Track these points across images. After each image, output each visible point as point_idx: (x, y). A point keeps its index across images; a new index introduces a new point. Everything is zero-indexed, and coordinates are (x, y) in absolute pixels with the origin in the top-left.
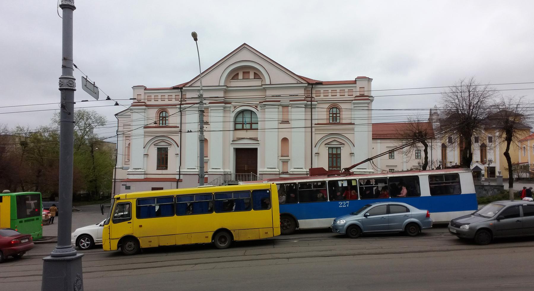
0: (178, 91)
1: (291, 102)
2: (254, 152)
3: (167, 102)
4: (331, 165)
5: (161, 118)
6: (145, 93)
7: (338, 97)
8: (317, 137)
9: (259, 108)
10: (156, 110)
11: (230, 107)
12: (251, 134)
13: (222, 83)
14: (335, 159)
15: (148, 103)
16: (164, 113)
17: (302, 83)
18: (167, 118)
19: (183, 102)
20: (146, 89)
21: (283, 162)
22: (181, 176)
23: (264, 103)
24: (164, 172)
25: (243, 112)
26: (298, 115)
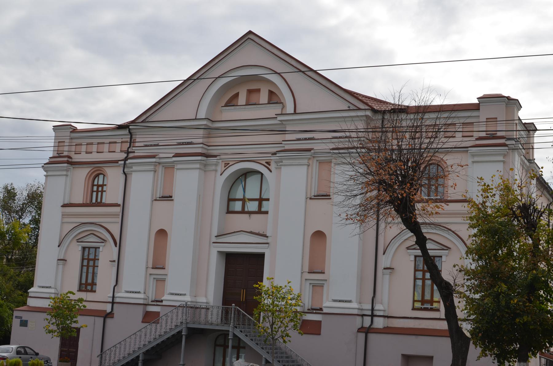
4: (418, 297)
5: (95, 188)
9: (273, 166)
11: (216, 165)
13: (202, 114)
15: (77, 158)
16: (101, 177)
17: (359, 109)
19: (131, 155)
20: (75, 130)
22: (115, 305)
25: (245, 174)
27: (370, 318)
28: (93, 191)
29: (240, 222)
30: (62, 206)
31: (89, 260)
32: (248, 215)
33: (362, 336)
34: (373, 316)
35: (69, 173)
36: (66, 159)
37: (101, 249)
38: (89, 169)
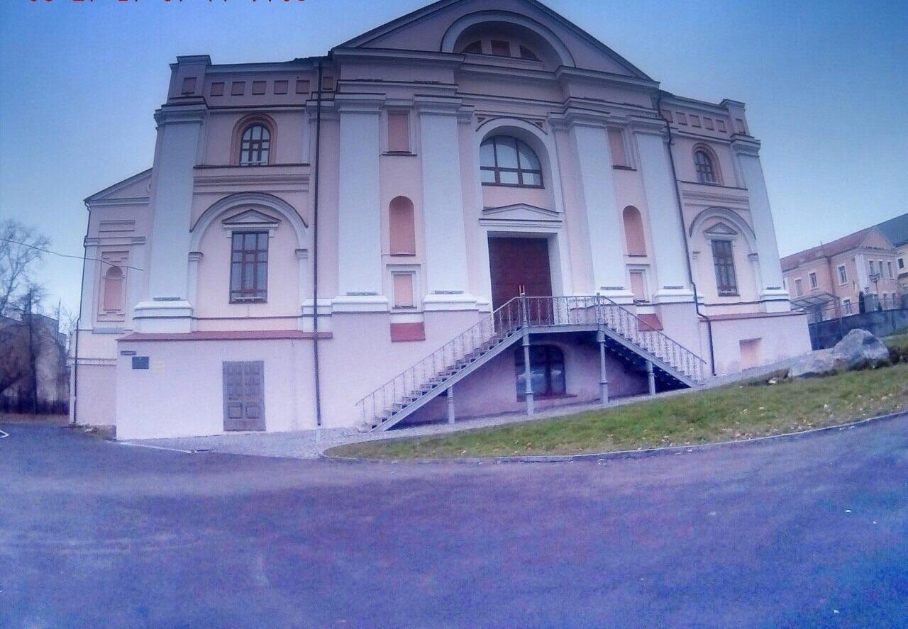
1: (635, 119)
3: (269, 99)
5: (246, 146)
6: (207, 75)
8: (689, 215)
10: (238, 118)
14: (723, 268)
18: (265, 145)
21: (633, 273)
22: (321, 321)
24: (255, 310)
28: (242, 150)
29: (501, 197)
31: (245, 252)
33: (704, 326)
36: (201, 100)
37: (271, 233)
38: (241, 116)
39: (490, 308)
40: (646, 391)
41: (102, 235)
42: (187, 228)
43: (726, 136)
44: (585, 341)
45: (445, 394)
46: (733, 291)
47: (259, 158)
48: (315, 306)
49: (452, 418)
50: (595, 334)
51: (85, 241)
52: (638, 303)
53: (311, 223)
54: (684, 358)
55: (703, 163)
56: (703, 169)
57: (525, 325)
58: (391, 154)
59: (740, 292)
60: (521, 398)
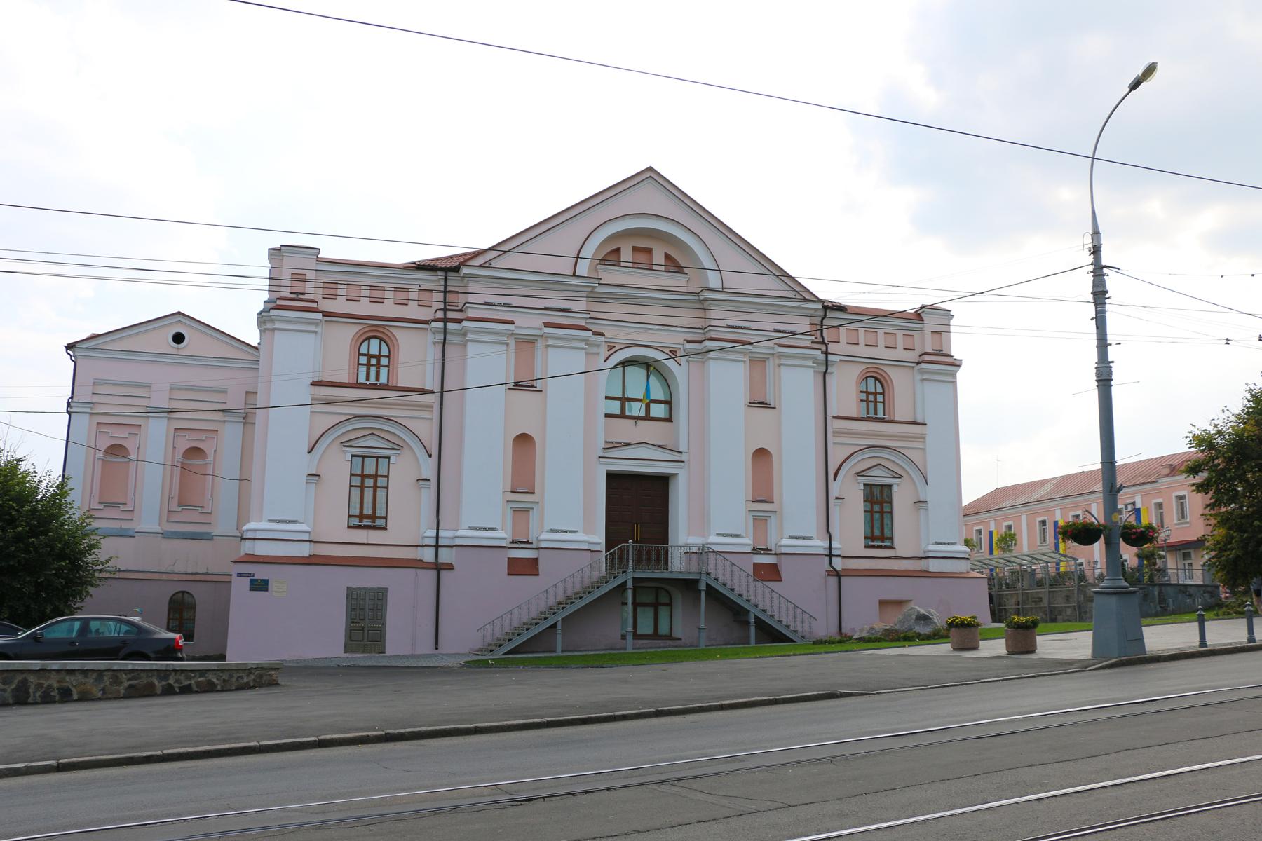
0: (432, 281)
1: (781, 349)
2: (661, 483)
3: (388, 309)
5: (363, 360)
7: (880, 352)
10: (355, 329)
12: (647, 431)
14: (877, 516)
18: (384, 361)
23: (703, 345)
24: (374, 536)
26: (796, 385)
27: (827, 559)
29: (625, 431)
30: (314, 384)
31: (363, 476)
32: (633, 421)
33: (834, 580)
34: (830, 556)
35: (319, 330)
38: (360, 327)
39: (603, 547)
40: (749, 643)
41: (96, 399)
42: (306, 450)
43: (913, 356)
44: (689, 585)
45: (554, 626)
46: (887, 543)
47: (378, 379)
48: (437, 537)
49: (559, 648)
50: (696, 582)
51: (69, 403)
52: (756, 551)
53: (435, 453)
54: (791, 612)
55: (871, 389)
56: (871, 398)
57: (630, 569)
58: (518, 386)
59: (896, 545)
60: (624, 637)
